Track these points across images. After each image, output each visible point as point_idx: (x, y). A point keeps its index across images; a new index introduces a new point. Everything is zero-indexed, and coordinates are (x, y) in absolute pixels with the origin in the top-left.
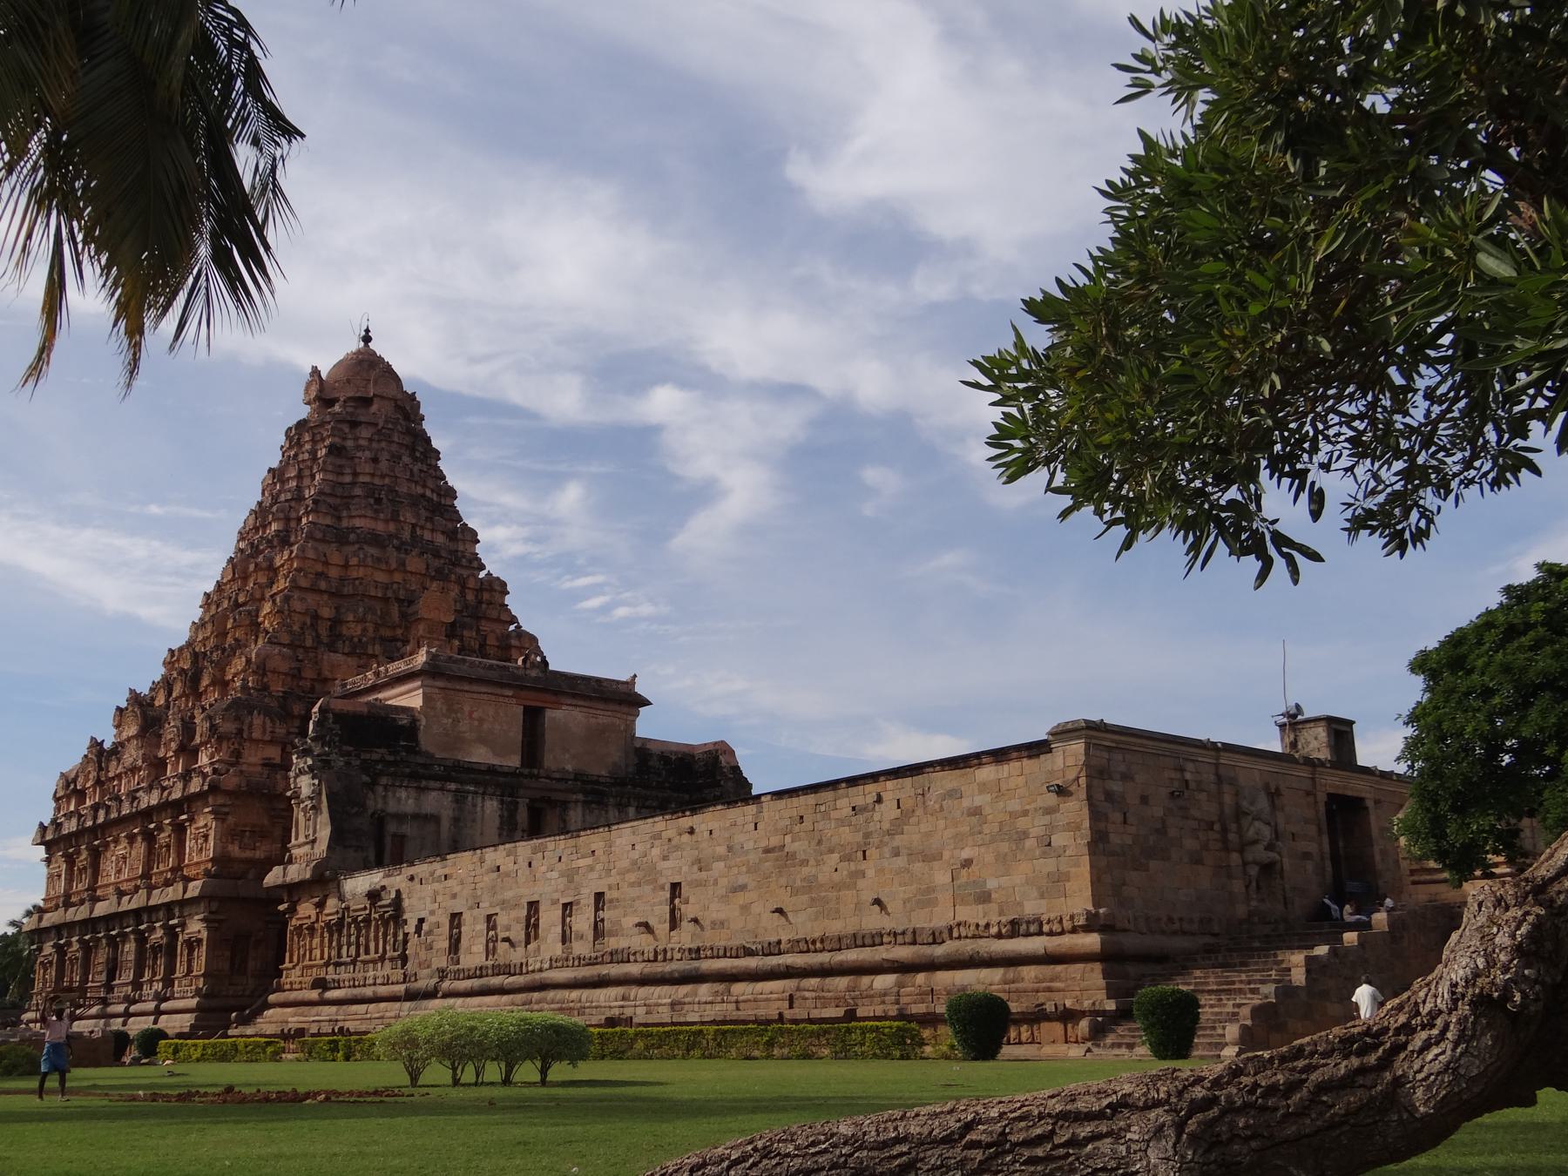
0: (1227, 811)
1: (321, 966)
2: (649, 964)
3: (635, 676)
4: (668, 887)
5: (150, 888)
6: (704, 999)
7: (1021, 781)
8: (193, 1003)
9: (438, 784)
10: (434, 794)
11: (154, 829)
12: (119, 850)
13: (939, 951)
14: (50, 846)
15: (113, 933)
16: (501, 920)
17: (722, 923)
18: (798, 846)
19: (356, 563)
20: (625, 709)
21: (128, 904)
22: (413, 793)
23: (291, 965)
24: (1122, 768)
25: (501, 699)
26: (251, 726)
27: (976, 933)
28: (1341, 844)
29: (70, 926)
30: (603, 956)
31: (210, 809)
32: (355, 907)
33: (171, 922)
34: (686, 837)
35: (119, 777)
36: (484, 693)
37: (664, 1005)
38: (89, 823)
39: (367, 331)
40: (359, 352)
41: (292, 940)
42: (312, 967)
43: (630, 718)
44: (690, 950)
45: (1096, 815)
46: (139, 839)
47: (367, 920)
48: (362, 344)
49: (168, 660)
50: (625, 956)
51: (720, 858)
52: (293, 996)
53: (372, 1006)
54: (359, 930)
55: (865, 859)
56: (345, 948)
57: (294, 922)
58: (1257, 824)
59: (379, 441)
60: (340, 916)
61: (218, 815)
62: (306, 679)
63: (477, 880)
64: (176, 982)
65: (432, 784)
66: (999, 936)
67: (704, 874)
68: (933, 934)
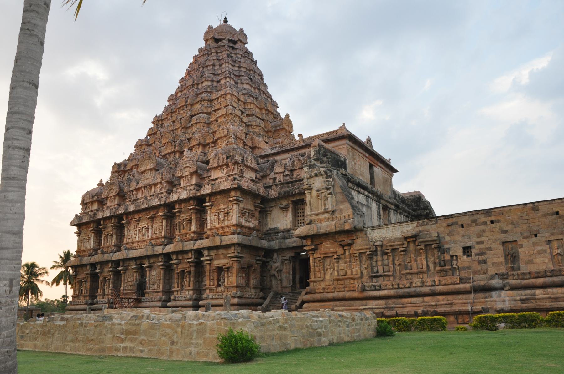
12: (141, 225)
15: (145, 266)
19: (250, 101)
25: (364, 157)
26: (247, 159)
29: (103, 264)
31: (235, 198)
32: (388, 244)
33: (202, 259)
35: (137, 190)
36: (362, 153)
39: (226, 18)
42: (344, 279)
48: (222, 23)
52: (330, 295)
59: (244, 57)
60: (373, 249)
61: (238, 201)
62: (247, 145)
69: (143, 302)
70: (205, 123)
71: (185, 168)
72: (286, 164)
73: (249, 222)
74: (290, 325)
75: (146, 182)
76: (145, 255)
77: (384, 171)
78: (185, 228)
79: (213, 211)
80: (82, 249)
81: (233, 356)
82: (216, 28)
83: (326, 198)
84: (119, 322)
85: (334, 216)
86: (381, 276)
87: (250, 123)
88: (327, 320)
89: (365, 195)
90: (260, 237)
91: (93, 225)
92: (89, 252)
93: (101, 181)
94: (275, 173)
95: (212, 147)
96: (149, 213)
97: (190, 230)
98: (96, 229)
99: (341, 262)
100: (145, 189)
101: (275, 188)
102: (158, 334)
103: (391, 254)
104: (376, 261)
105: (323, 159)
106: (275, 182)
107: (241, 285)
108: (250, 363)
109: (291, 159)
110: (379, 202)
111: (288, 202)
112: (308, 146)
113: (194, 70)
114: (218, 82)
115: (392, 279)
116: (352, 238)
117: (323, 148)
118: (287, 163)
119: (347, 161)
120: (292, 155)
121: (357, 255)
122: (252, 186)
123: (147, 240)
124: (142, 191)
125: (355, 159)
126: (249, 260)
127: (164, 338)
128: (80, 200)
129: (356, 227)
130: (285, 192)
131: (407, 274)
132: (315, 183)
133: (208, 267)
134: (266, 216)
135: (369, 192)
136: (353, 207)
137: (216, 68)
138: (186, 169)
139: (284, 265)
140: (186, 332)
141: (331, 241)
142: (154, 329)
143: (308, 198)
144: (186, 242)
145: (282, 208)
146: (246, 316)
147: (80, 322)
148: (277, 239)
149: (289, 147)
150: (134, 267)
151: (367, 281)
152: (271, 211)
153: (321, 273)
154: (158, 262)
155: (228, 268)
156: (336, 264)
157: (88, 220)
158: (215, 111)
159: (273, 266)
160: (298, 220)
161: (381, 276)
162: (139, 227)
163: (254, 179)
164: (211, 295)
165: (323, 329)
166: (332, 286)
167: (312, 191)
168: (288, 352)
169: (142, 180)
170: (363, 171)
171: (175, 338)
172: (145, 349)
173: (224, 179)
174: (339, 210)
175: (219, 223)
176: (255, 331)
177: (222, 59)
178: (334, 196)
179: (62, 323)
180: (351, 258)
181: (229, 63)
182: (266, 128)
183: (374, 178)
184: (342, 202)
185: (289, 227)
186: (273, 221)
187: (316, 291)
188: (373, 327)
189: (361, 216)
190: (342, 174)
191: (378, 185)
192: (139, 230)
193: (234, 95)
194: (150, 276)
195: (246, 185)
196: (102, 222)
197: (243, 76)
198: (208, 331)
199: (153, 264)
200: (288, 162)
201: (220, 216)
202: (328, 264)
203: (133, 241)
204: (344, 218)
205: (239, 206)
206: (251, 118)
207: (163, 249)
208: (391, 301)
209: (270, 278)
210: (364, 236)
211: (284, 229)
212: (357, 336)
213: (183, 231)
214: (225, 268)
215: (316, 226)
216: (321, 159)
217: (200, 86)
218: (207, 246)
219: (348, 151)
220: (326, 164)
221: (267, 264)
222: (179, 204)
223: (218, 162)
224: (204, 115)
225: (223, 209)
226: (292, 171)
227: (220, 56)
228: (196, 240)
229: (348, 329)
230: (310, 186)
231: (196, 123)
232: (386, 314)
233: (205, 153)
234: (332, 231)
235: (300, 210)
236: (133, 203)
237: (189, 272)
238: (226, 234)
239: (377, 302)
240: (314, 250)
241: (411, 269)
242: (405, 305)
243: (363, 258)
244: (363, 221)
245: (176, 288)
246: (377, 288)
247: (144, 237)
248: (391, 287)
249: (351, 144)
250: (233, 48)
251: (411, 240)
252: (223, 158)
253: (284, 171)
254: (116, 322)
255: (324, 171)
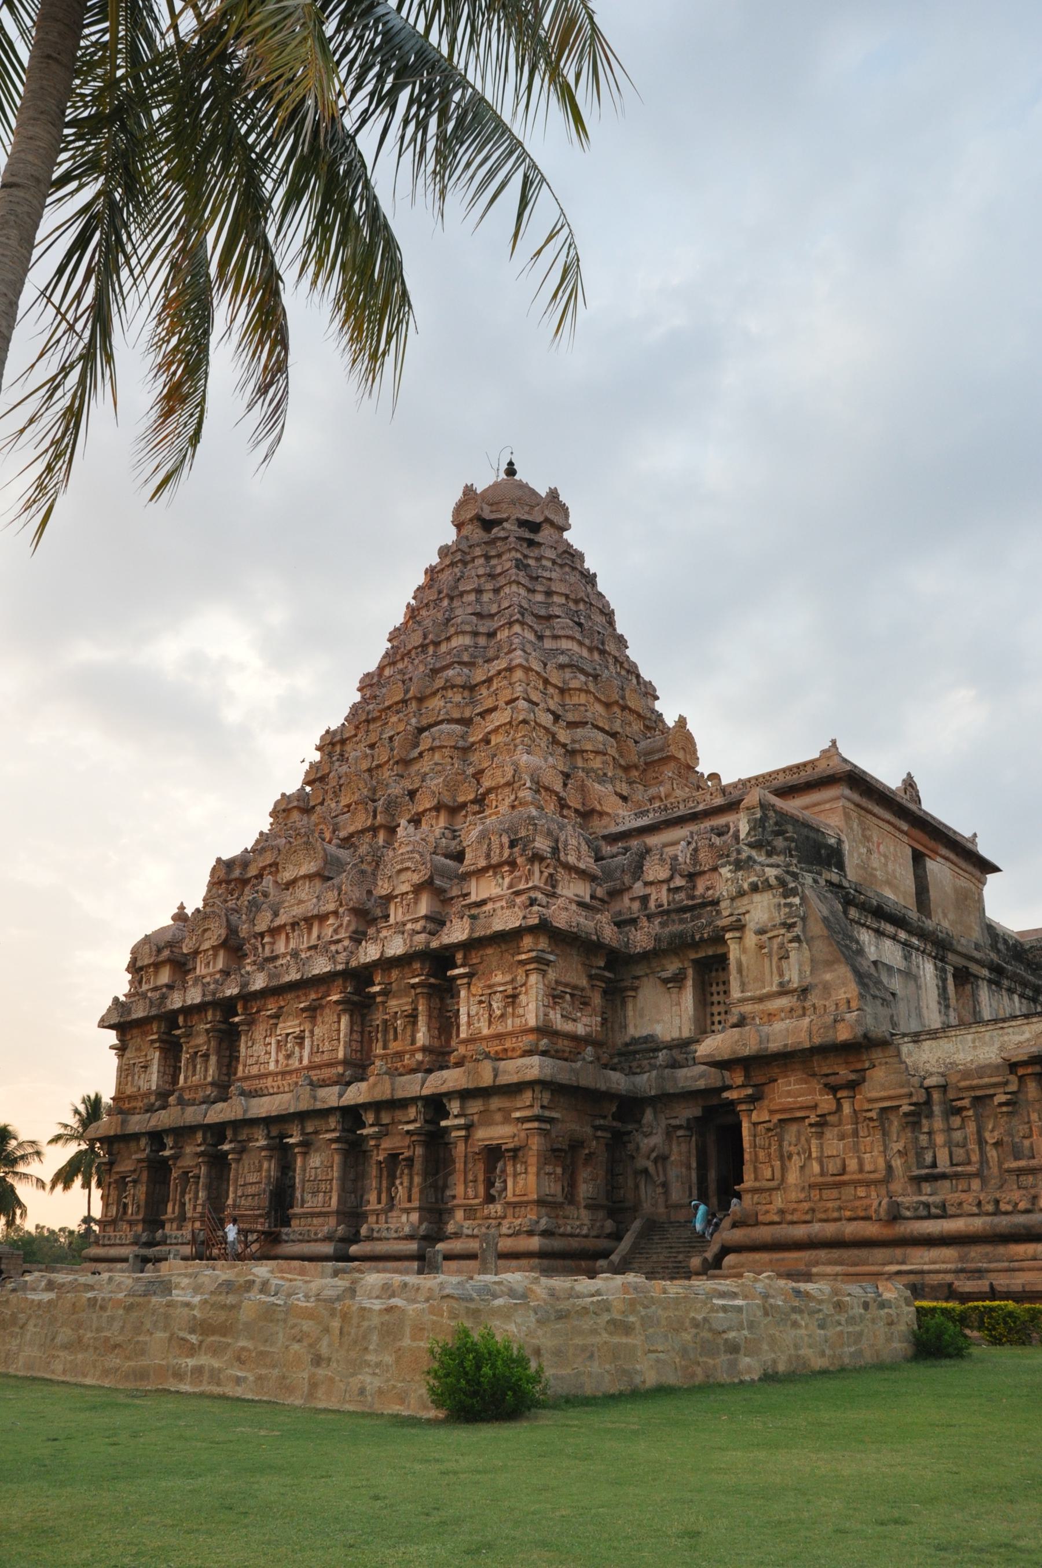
8: (535, 1243)
12: (284, 1028)
15: (291, 1141)
19: (578, 686)
26: (566, 845)
31: (533, 954)
32: (963, 1084)
33: (443, 1123)
36: (888, 822)
48: (503, 476)
49: (283, 807)
52: (800, 1232)
59: (561, 566)
60: (920, 1097)
61: (541, 963)
62: (569, 807)
69: (286, 1242)
70: (455, 747)
71: (400, 871)
72: (675, 858)
73: (574, 1020)
74: (642, 1317)
75: (298, 911)
76: (292, 1111)
77: (957, 870)
78: (400, 1037)
79: (473, 990)
80: (128, 1092)
81: (469, 1401)
82: (486, 490)
83: (783, 953)
84: (187, 1299)
85: (808, 1004)
86: (944, 1176)
87: (577, 746)
88: (758, 1306)
89: (899, 941)
90: (604, 1061)
91: (159, 1027)
92: (146, 1101)
93: (182, 907)
94: (647, 884)
95: (474, 814)
96: (306, 995)
97: (413, 1042)
98: (165, 1037)
99: (830, 1134)
100: (294, 931)
101: (646, 924)
102: (281, 1335)
103: (970, 1113)
104: (929, 1133)
105: (775, 843)
106: (646, 908)
107: (550, 1199)
108: (513, 1425)
109: (689, 843)
110: (942, 960)
111: (682, 962)
112: (732, 806)
113: (427, 605)
114: (492, 635)
115: (976, 1184)
116: (859, 1066)
117: (775, 811)
118: (679, 854)
119: (846, 846)
120: (692, 833)
121: (873, 1114)
122: (582, 920)
123: (297, 1070)
124: (287, 934)
125: (868, 839)
126: (574, 1126)
127: (296, 1347)
128: (127, 959)
129: (869, 1035)
130: (673, 936)
131: (1020, 1172)
132: (752, 911)
133: (461, 1147)
134: (624, 1003)
135: (910, 932)
136: (861, 978)
137: (486, 597)
138: (404, 876)
139: (674, 1142)
140: (353, 1331)
141: (800, 1075)
142: (272, 1321)
143: (734, 952)
144: (401, 1075)
145: (665, 981)
146: (520, 1290)
147: (90, 1295)
148: (653, 1067)
149: (682, 811)
150: (262, 1142)
151: (904, 1189)
152: (635, 989)
153: (772, 1167)
154: (327, 1131)
155: (516, 1150)
156: (814, 1142)
157: (145, 1014)
158: (482, 715)
159: (641, 1145)
160: (712, 1015)
161: (944, 1176)
162: (278, 1032)
163: (587, 899)
164: (468, 1226)
165: (745, 1332)
166: (806, 1206)
167: (743, 932)
168: (636, 1395)
169: (286, 904)
170: (894, 871)
171: (324, 1349)
172: (248, 1375)
173: (504, 903)
174: (820, 987)
175: (490, 1023)
176: (540, 1332)
177: (500, 574)
178: (805, 945)
179: (47, 1296)
180: (857, 1123)
181: (519, 583)
182: (622, 756)
183: (928, 891)
184: (829, 964)
185: (686, 1034)
186: (642, 1016)
187: (761, 1218)
188: (903, 1328)
189: (885, 1002)
190: (829, 883)
191: (940, 911)
192: (278, 1042)
193: (532, 670)
194: (304, 1170)
195: (562, 917)
196: (181, 1020)
197: (558, 617)
198: (408, 1331)
199: (313, 1137)
200: (682, 852)
201: (495, 1005)
202: (794, 1140)
203: (262, 1071)
204: (833, 1008)
205: (544, 976)
206: (580, 732)
207: (341, 1096)
208: (975, 1252)
209: (636, 1178)
210: (896, 1059)
211: (673, 1040)
212: (852, 1355)
213: (394, 1046)
214: (507, 1150)
215: (758, 1031)
216: (769, 843)
217: (444, 648)
218: (458, 1088)
219: (847, 816)
220: (782, 858)
221: (626, 1138)
222: (383, 970)
223: (488, 856)
224: (454, 726)
225: (503, 984)
226: (692, 877)
227: (494, 567)
228: (429, 1071)
229: (822, 1332)
230: (739, 920)
231: (432, 749)
232: (960, 1290)
233: (455, 831)
234: (800, 1047)
235: (717, 984)
236: (261, 969)
237: (410, 1160)
238: (510, 1054)
239: (935, 1253)
240: (754, 1099)
241: (1034, 1157)
242: (1016, 1264)
243: (891, 1123)
244: (892, 1016)
245: (373, 1206)
246: (934, 1210)
247: (290, 1062)
248: (975, 1210)
249: (856, 797)
250: (531, 543)
251: (1029, 1071)
252: (502, 846)
253: (672, 878)
254: (179, 1298)
255: (777, 878)
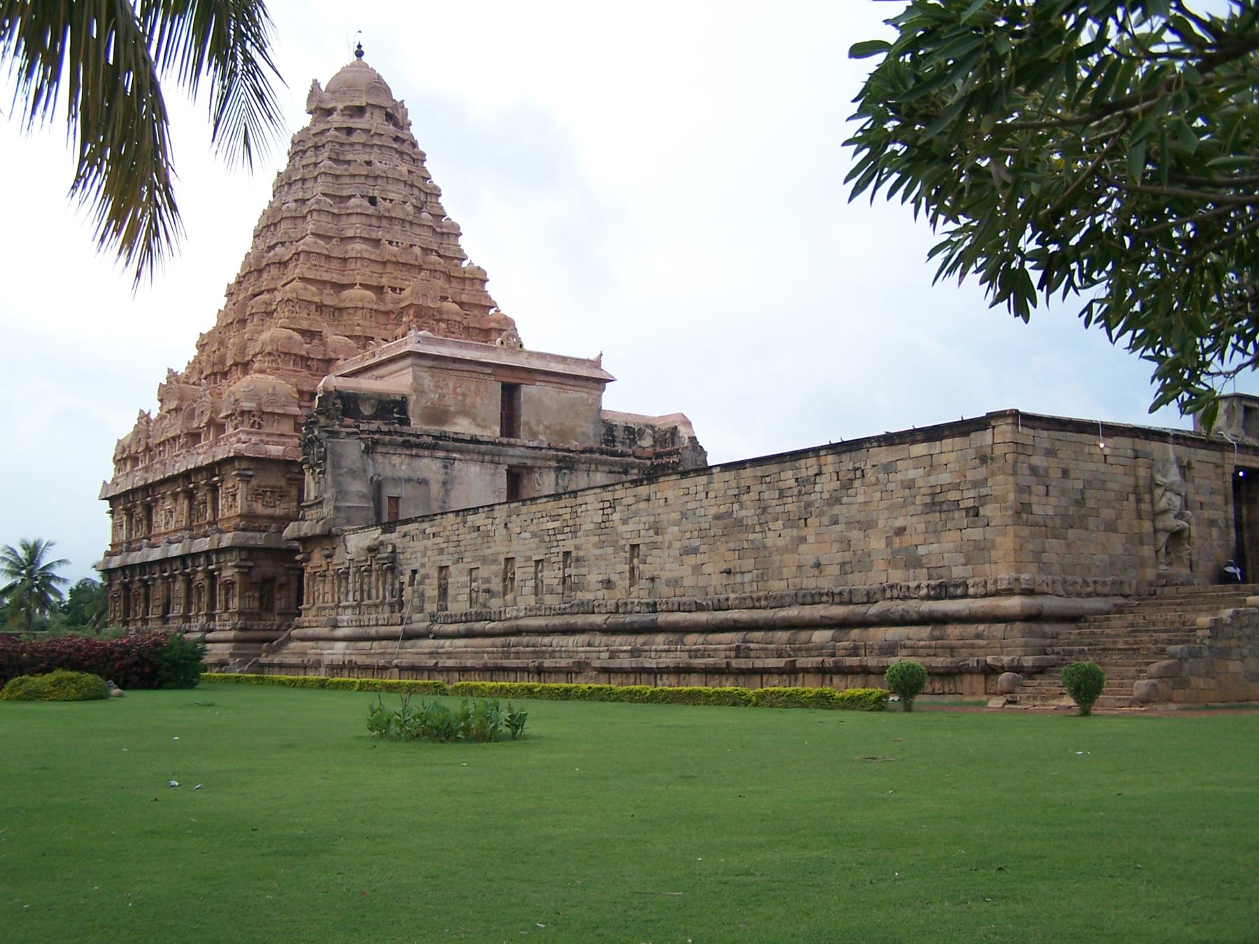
0: (1141, 482)
1: (332, 609)
2: (612, 616)
3: (601, 355)
4: (627, 548)
5: (192, 538)
6: (660, 648)
7: (952, 456)
8: (231, 635)
9: (427, 453)
10: (425, 461)
11: (193, 488)
13: (873, 610)
14: (113, 500)
15: (166, 574)
16: (484, 572)
17: (676, 582)
18: (748, 514)
20: (591, 384)
21: (176, 550)
22: (407, 460)
23: (308, 606)
24: (1047, 444)
25: (482, 376)
27: (907, 594)
28: (1244, 511)
29: (132, 567)
30: (571, 607)
33: (210, 567)
34: (643, 505)
37: (625, 651)
38: (142, 483)
39: (359, 46)
40: (353, 65)
41: (308, 585)
42: (325, 608)
43: (598, 393)
44: (647, 604)
45: (1021, 489)
46: (181, 496)
47: (369, 570)
48: (355, 58)
50: (591, 607)
51: (677, 523)
52: (310, 632)
53: (375, 644)
54: (362, 578)
55: (806, 526)
56: (351, 594)
57: (309, 570)
58: (1168, 494)
61: (246, 479)
63: (461, 537)
64: (217, 618)
65: (421, 452)
66: (928, 597)
67: (660, 538)
68: (868, 594)
87: (342, 305)
99: (329, 579)
114: (305, 217)
137: (309, 184)
